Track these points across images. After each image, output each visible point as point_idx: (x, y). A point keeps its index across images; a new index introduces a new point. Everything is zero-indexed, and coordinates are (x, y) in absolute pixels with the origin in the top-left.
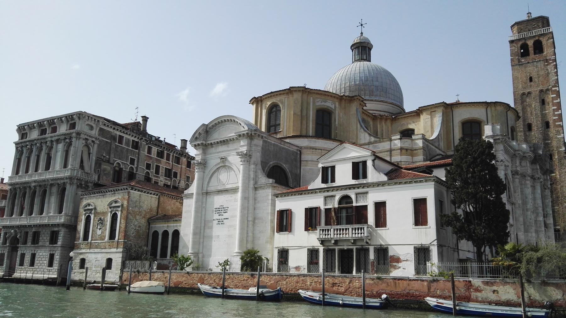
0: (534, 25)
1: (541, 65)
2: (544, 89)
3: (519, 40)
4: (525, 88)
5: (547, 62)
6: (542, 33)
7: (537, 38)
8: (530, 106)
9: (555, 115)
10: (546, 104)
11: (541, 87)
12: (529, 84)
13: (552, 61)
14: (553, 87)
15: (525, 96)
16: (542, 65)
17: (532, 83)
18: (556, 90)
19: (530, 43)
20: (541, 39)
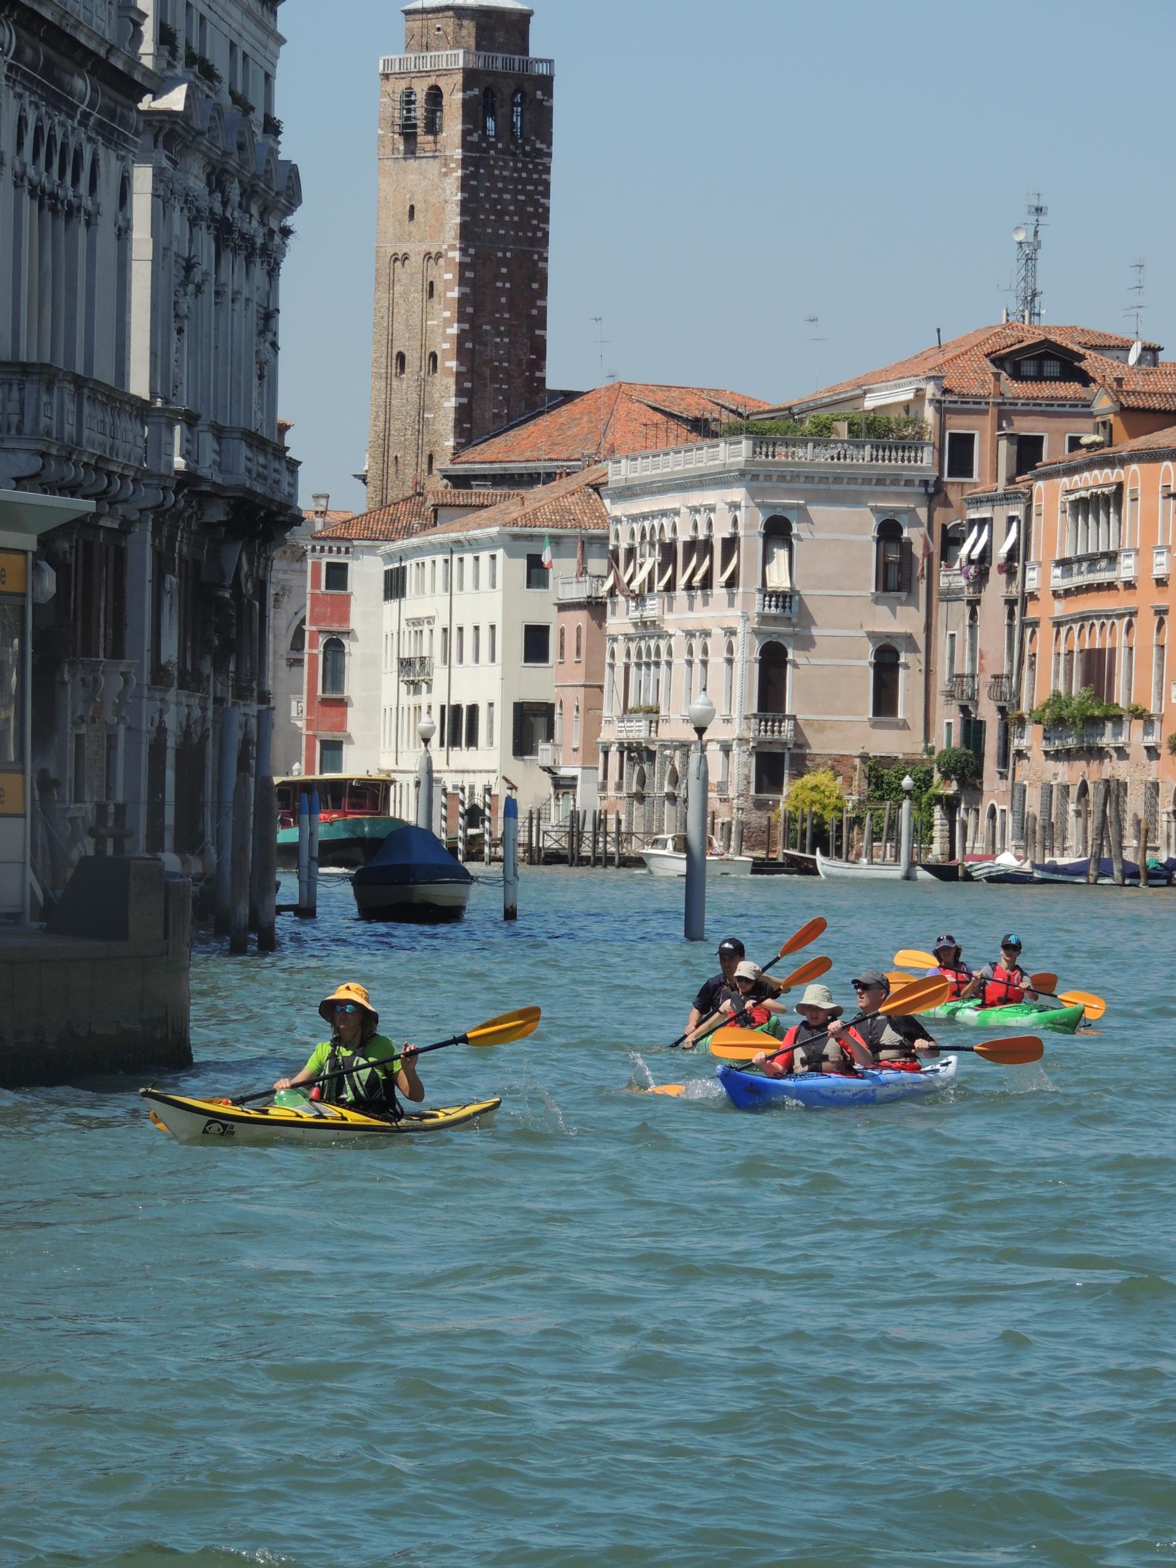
0: (439, 29)
1: (432, 168)
2: (434, 251)
3: (401, 75)
4: (399, 240)
5: (446, 165)
6: (445, 67)
7: (432, 81)
8: (405, 295)
9: (446, 338)
10: (436, 297)
11: (425, 247)
12: (407, 229)
13: (453, 165)
14: (452, 247)
15: (398, 264)
16: (436, 172)
17: (412, 227)
18: (454, 258)
19: (421, 90)
20: (442, 83)
